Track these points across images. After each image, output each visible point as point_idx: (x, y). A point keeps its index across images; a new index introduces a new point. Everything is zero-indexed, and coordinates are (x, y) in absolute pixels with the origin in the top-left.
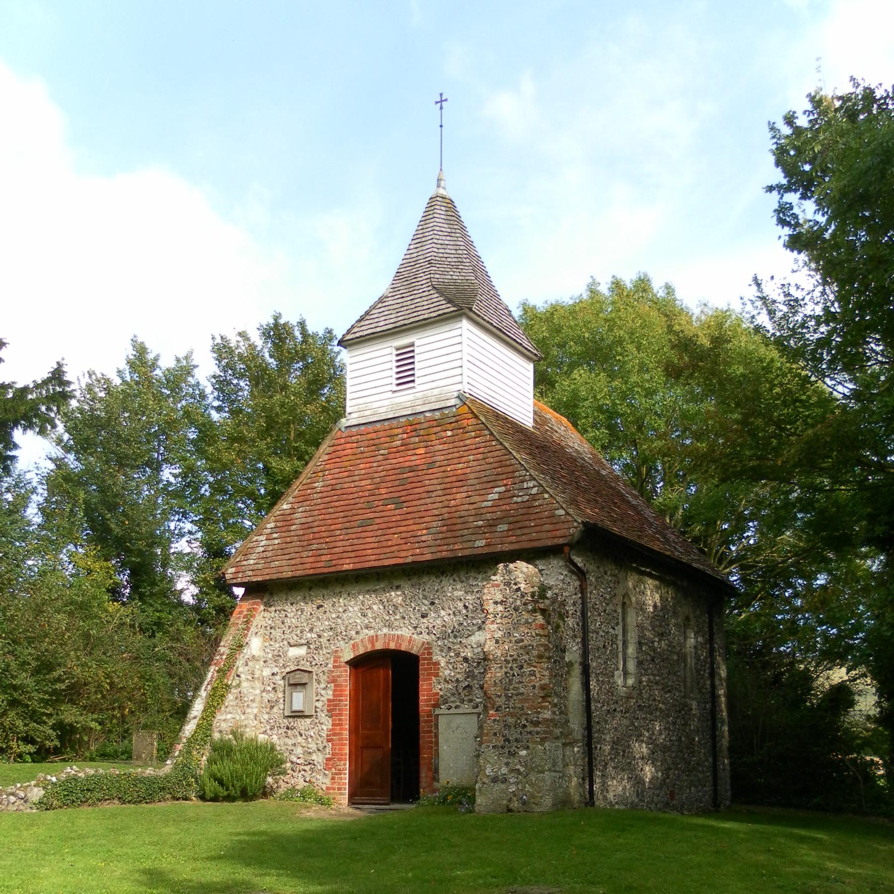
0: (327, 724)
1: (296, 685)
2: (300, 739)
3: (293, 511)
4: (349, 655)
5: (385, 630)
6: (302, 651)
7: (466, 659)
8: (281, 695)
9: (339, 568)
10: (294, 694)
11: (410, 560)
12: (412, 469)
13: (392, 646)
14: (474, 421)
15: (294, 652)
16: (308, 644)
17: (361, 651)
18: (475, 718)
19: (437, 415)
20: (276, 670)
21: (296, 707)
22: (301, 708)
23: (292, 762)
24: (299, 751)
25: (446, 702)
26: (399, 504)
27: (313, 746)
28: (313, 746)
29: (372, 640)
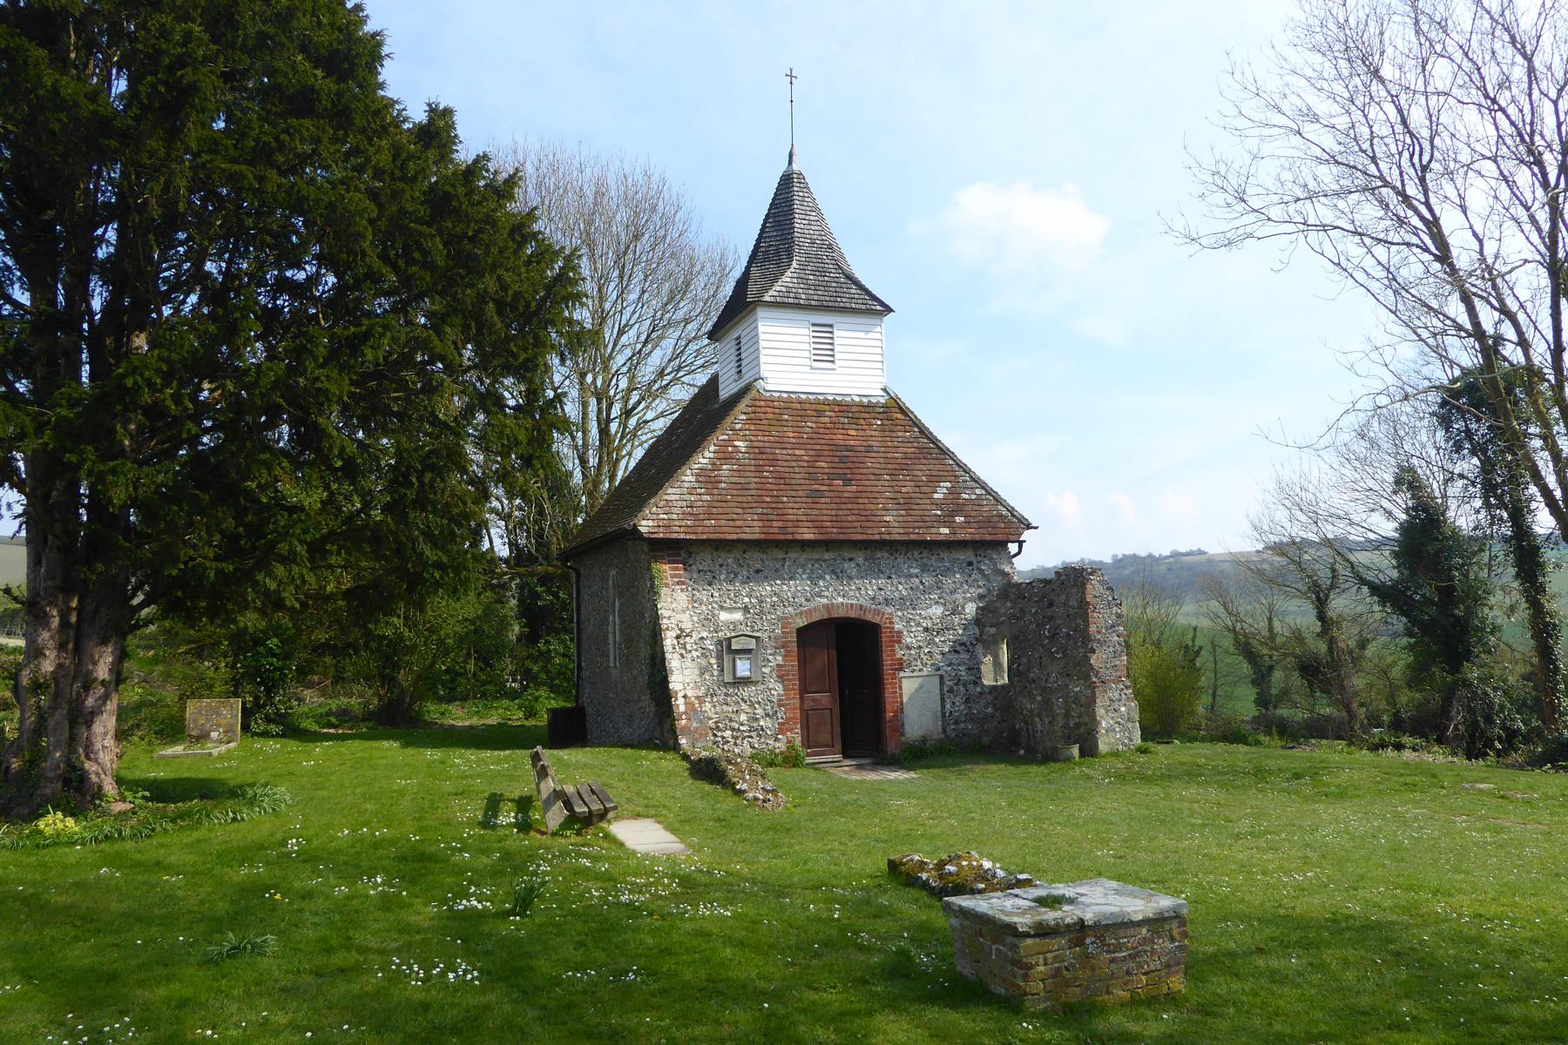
0: (777, 689)
1: (738, 652)
2: (744, 707)
3: (715, 467)
4: (801, 622)
5: (840, 600)
6: (738, 616)
7: (926, 629)
8: (713, 661)
9: (798, 537)
10: (738, 662)
11: (877, 537)
12: (849, 449)
13: (853, 614)
14: (900, 416)
15: (724, 616)
16: (746, 609)
17: (816, 617)
18: (937, 680)
19: (865, 400)
20: (704, 634)
21: (740, 674)
22: (747, 673)
23: (733, 730)
24: (743, 717)
25: (909, 665)
26: (847, 482)
27: (760, 711)
28: (760, 711)
29: (826, 607)
